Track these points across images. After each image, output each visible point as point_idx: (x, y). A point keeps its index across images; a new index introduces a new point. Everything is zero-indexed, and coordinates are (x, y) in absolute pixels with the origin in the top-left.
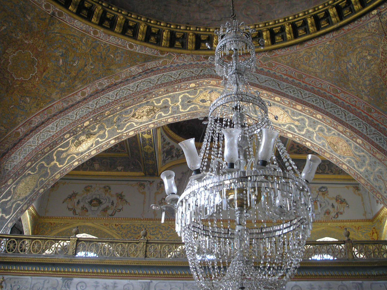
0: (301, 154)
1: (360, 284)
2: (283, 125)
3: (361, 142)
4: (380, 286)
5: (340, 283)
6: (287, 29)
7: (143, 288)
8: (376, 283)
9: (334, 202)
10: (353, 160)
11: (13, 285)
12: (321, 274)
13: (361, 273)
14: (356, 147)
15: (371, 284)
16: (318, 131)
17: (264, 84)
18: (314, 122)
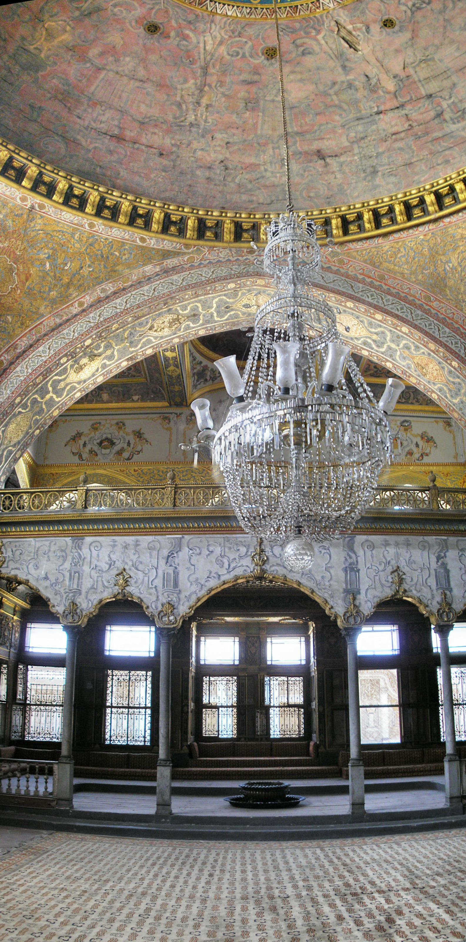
3: (457, 366)
5: (421, 538)
10: (445, 388)
12: (398, 527)
14: (450, 372)
16: (403, 348)
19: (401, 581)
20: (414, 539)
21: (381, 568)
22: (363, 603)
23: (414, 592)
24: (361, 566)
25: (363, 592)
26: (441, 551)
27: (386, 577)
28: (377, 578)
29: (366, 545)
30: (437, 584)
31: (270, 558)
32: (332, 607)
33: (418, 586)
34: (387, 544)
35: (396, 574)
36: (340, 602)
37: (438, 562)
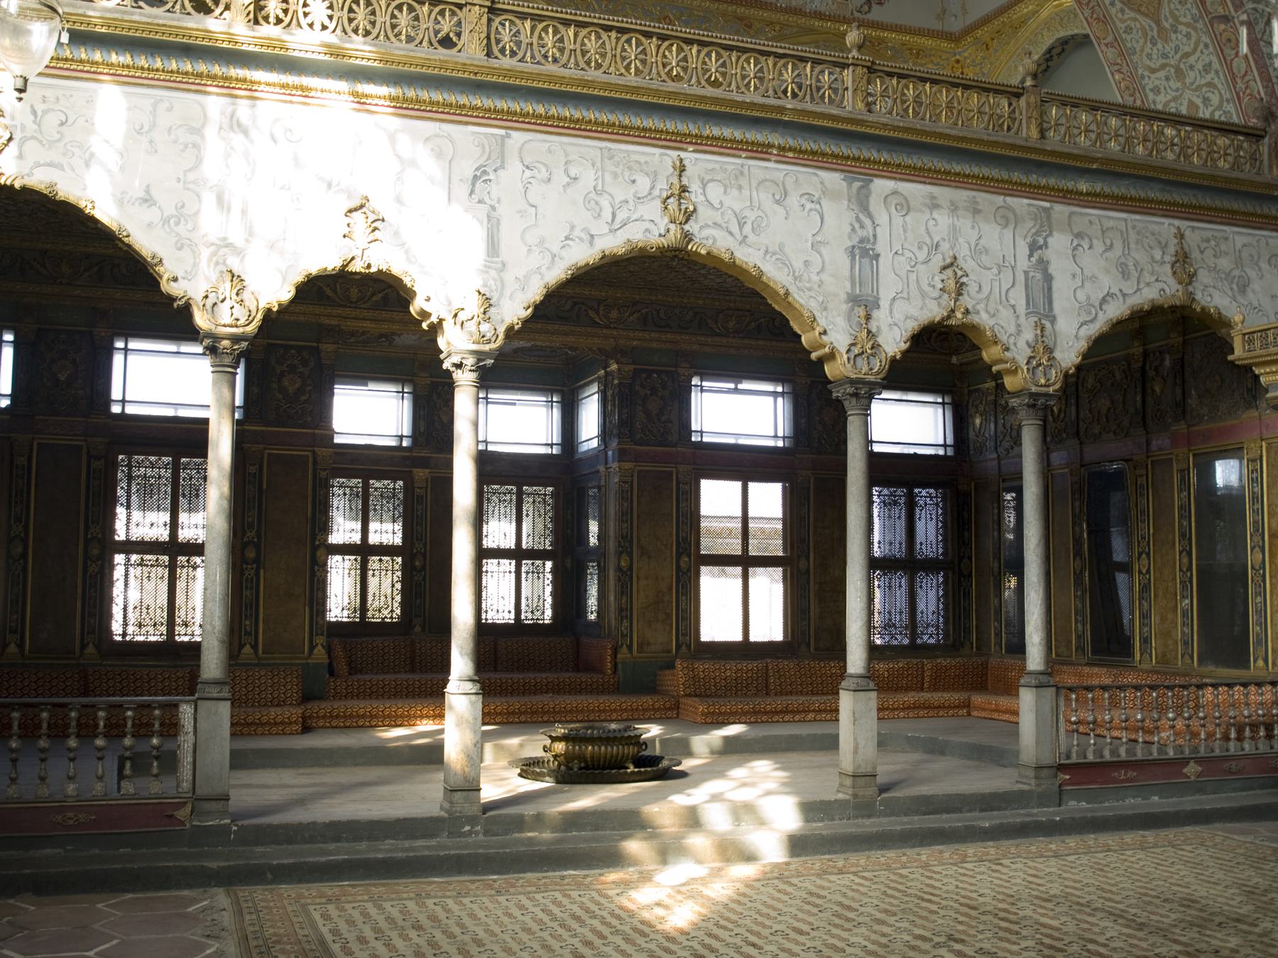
1: (1045, 209)
4: (1091, 222)
5: (999, 200)
7: (484, 152)
8: (1081, 214)
11: (40, 108)
13: (1052, 181)
15: (1071, 214)
19: (960, 288)
20: (988, 200)
21: (922, 255)
22: (885, 329)
23: (984, 315)
24: (881, 247)
25: (885, 303)
26: (1037, 234)
27: (930, 277)
28: (913, 277)
29: (894, 201)
30: (1028, 304)
31: (700, 209)
32: (825, 332)
33: (992, 305)
34: (934, 205)
35: (949, 272)
36: (841, 322)
37: (1031, 255)
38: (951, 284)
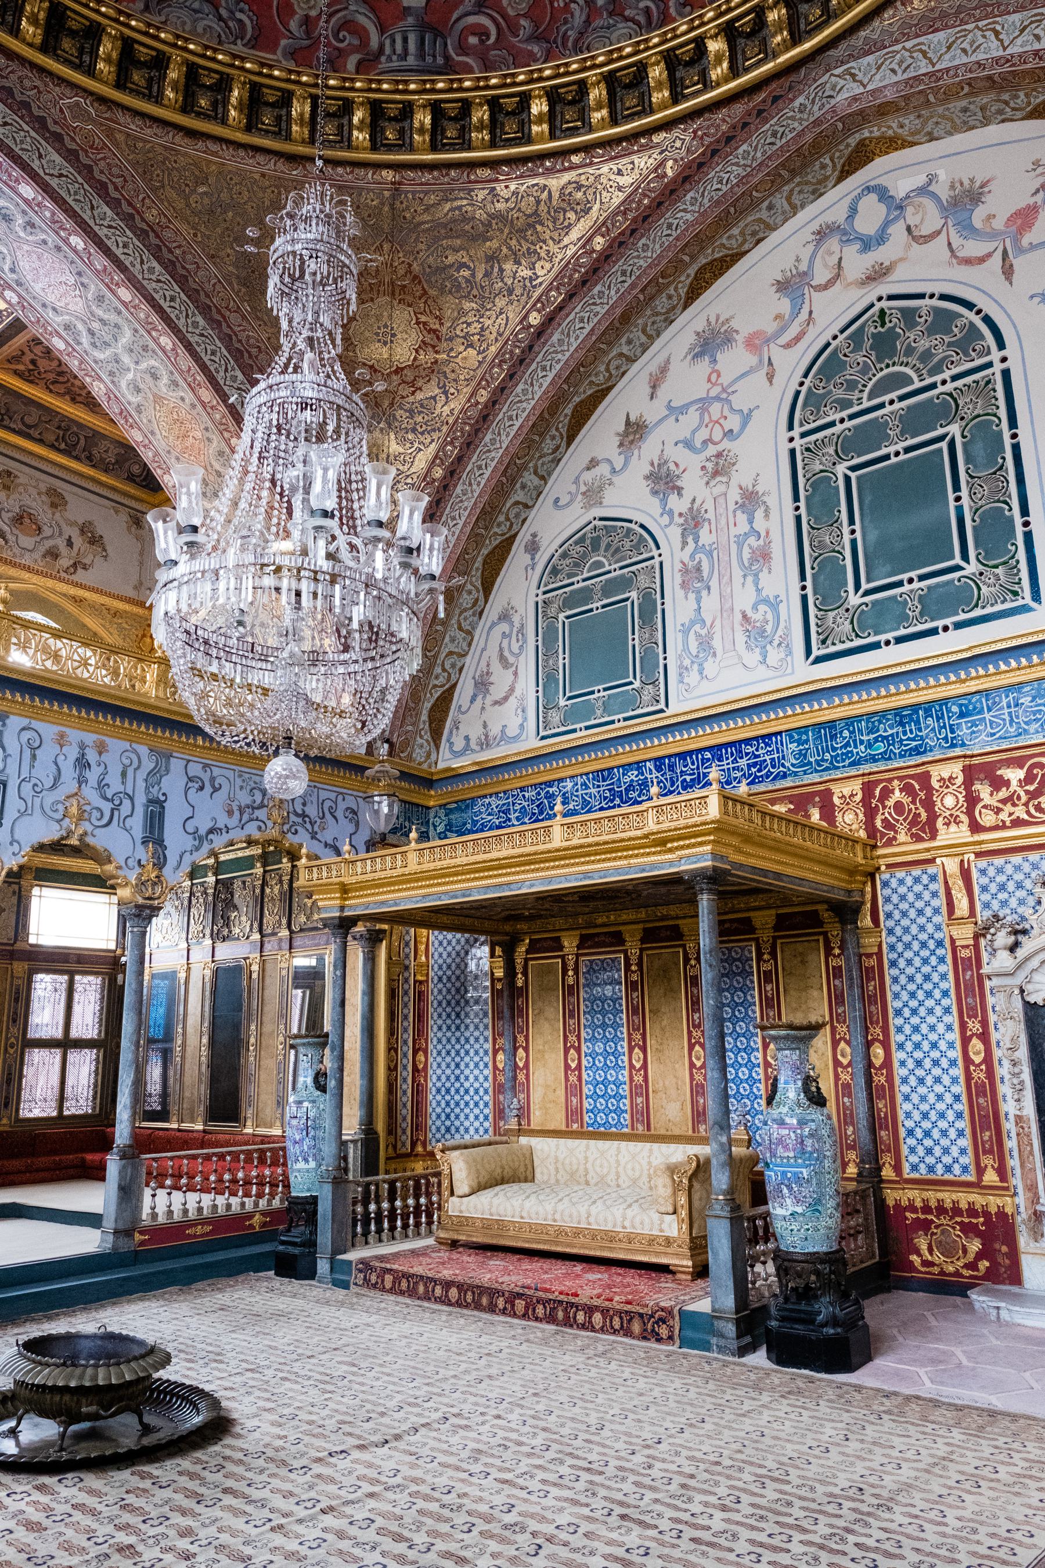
0: (31, 382)
2: (54, 309)
6: (173, 74)
9: (75, 533)
17: (54, 182)
18: (145, 348)
28: (37, 801)
38: (74, 810)
